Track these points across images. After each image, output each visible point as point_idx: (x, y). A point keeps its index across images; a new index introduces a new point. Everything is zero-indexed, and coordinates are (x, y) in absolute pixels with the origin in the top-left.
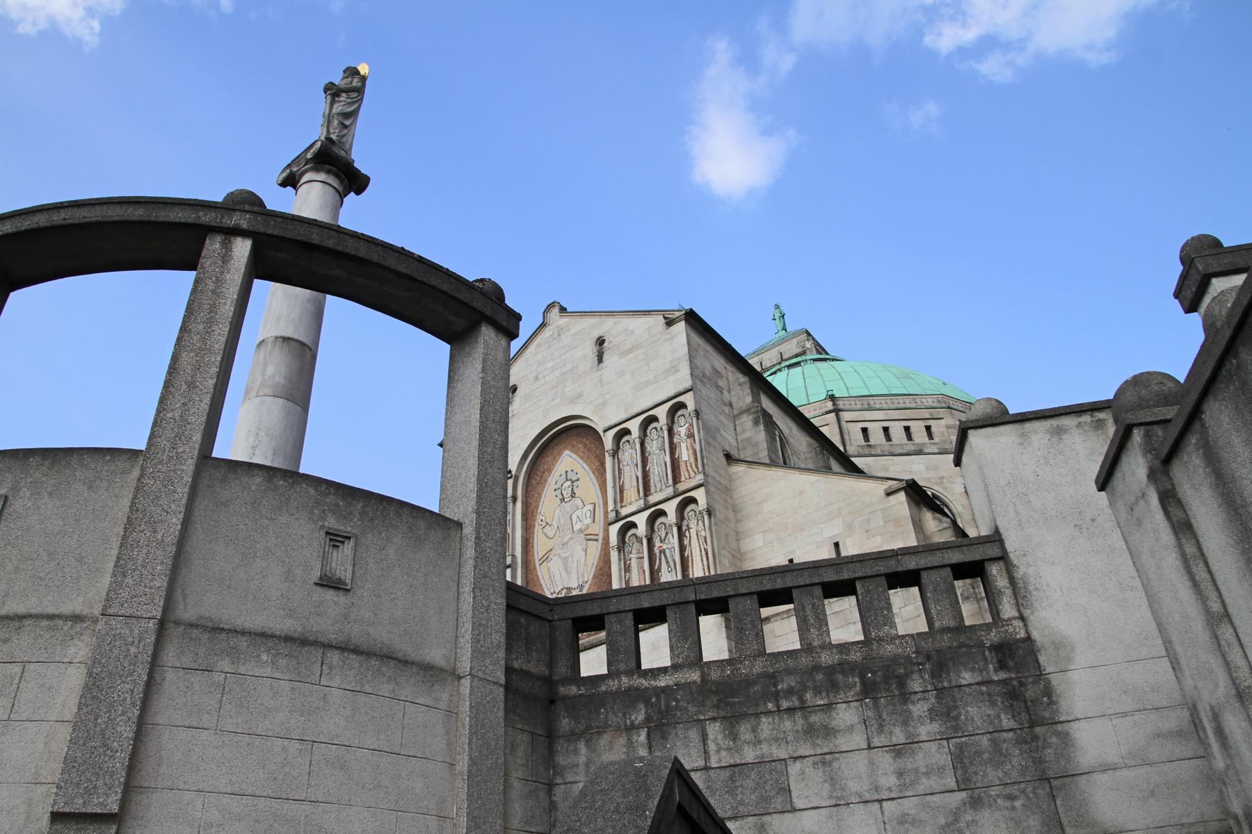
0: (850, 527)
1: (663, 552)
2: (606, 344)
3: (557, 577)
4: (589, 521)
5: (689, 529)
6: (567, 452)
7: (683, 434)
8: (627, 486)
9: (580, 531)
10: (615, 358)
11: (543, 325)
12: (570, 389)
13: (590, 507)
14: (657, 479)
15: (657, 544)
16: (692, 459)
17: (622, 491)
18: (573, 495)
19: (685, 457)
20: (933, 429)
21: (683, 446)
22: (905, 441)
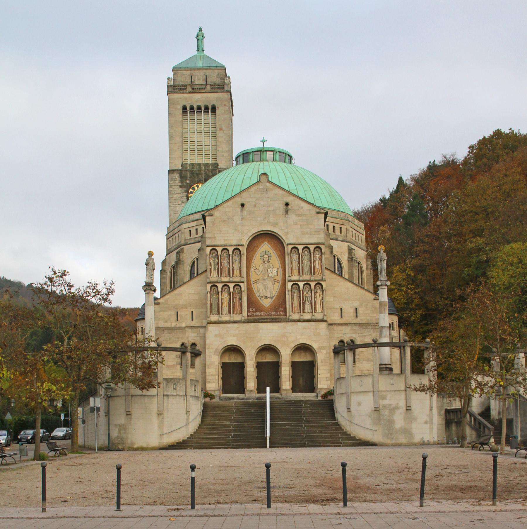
0: (361, 305)
1: (306, 297)
2: (289, 207)
3: (261, 291)
4: (275, 274)
5: (317, 292)
6: (266, 243)
7: (317, 258)
8: (294, 268)
9: (271, 277)
10: (293, 215)
11: (258, 182)
12: (272, 219)
13: (277, 269)
14: (306, 270)
15: (305, 294)
16: (320, 269)
17: (292, 269)
18: (268, 262)
19: (317, 266)
20: (342, 229)
21: (317, 262)
22: (332, 233)
